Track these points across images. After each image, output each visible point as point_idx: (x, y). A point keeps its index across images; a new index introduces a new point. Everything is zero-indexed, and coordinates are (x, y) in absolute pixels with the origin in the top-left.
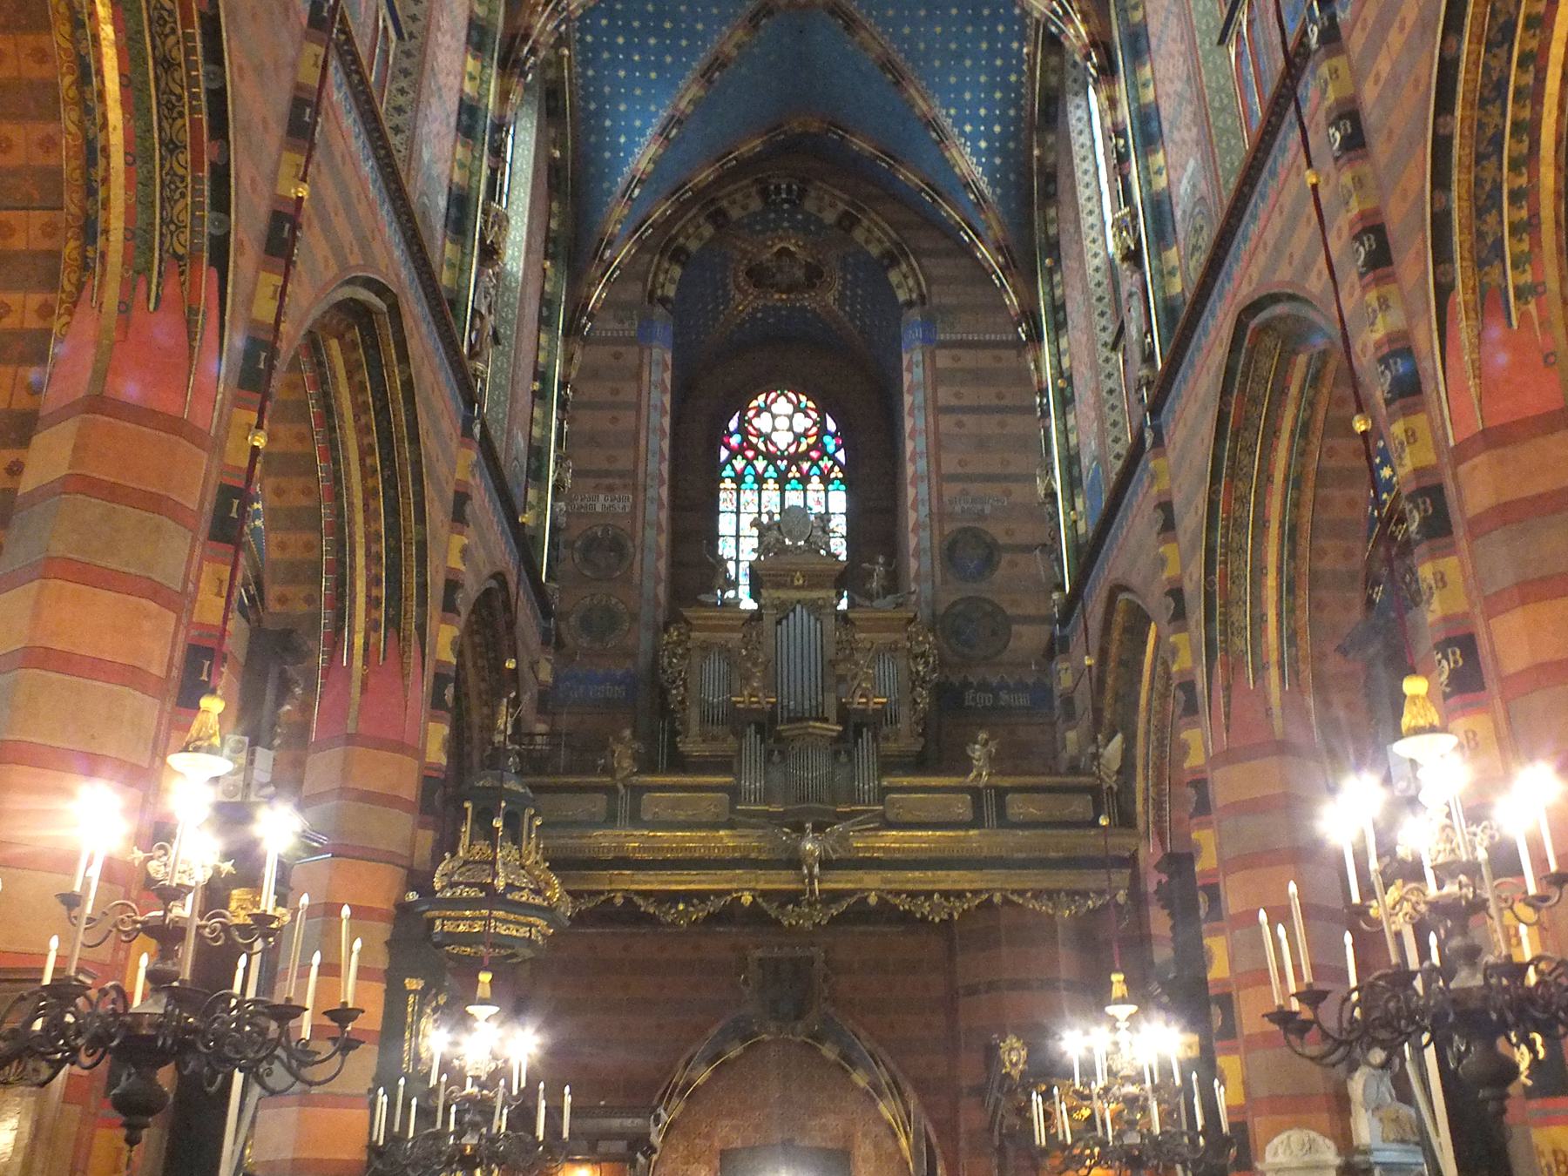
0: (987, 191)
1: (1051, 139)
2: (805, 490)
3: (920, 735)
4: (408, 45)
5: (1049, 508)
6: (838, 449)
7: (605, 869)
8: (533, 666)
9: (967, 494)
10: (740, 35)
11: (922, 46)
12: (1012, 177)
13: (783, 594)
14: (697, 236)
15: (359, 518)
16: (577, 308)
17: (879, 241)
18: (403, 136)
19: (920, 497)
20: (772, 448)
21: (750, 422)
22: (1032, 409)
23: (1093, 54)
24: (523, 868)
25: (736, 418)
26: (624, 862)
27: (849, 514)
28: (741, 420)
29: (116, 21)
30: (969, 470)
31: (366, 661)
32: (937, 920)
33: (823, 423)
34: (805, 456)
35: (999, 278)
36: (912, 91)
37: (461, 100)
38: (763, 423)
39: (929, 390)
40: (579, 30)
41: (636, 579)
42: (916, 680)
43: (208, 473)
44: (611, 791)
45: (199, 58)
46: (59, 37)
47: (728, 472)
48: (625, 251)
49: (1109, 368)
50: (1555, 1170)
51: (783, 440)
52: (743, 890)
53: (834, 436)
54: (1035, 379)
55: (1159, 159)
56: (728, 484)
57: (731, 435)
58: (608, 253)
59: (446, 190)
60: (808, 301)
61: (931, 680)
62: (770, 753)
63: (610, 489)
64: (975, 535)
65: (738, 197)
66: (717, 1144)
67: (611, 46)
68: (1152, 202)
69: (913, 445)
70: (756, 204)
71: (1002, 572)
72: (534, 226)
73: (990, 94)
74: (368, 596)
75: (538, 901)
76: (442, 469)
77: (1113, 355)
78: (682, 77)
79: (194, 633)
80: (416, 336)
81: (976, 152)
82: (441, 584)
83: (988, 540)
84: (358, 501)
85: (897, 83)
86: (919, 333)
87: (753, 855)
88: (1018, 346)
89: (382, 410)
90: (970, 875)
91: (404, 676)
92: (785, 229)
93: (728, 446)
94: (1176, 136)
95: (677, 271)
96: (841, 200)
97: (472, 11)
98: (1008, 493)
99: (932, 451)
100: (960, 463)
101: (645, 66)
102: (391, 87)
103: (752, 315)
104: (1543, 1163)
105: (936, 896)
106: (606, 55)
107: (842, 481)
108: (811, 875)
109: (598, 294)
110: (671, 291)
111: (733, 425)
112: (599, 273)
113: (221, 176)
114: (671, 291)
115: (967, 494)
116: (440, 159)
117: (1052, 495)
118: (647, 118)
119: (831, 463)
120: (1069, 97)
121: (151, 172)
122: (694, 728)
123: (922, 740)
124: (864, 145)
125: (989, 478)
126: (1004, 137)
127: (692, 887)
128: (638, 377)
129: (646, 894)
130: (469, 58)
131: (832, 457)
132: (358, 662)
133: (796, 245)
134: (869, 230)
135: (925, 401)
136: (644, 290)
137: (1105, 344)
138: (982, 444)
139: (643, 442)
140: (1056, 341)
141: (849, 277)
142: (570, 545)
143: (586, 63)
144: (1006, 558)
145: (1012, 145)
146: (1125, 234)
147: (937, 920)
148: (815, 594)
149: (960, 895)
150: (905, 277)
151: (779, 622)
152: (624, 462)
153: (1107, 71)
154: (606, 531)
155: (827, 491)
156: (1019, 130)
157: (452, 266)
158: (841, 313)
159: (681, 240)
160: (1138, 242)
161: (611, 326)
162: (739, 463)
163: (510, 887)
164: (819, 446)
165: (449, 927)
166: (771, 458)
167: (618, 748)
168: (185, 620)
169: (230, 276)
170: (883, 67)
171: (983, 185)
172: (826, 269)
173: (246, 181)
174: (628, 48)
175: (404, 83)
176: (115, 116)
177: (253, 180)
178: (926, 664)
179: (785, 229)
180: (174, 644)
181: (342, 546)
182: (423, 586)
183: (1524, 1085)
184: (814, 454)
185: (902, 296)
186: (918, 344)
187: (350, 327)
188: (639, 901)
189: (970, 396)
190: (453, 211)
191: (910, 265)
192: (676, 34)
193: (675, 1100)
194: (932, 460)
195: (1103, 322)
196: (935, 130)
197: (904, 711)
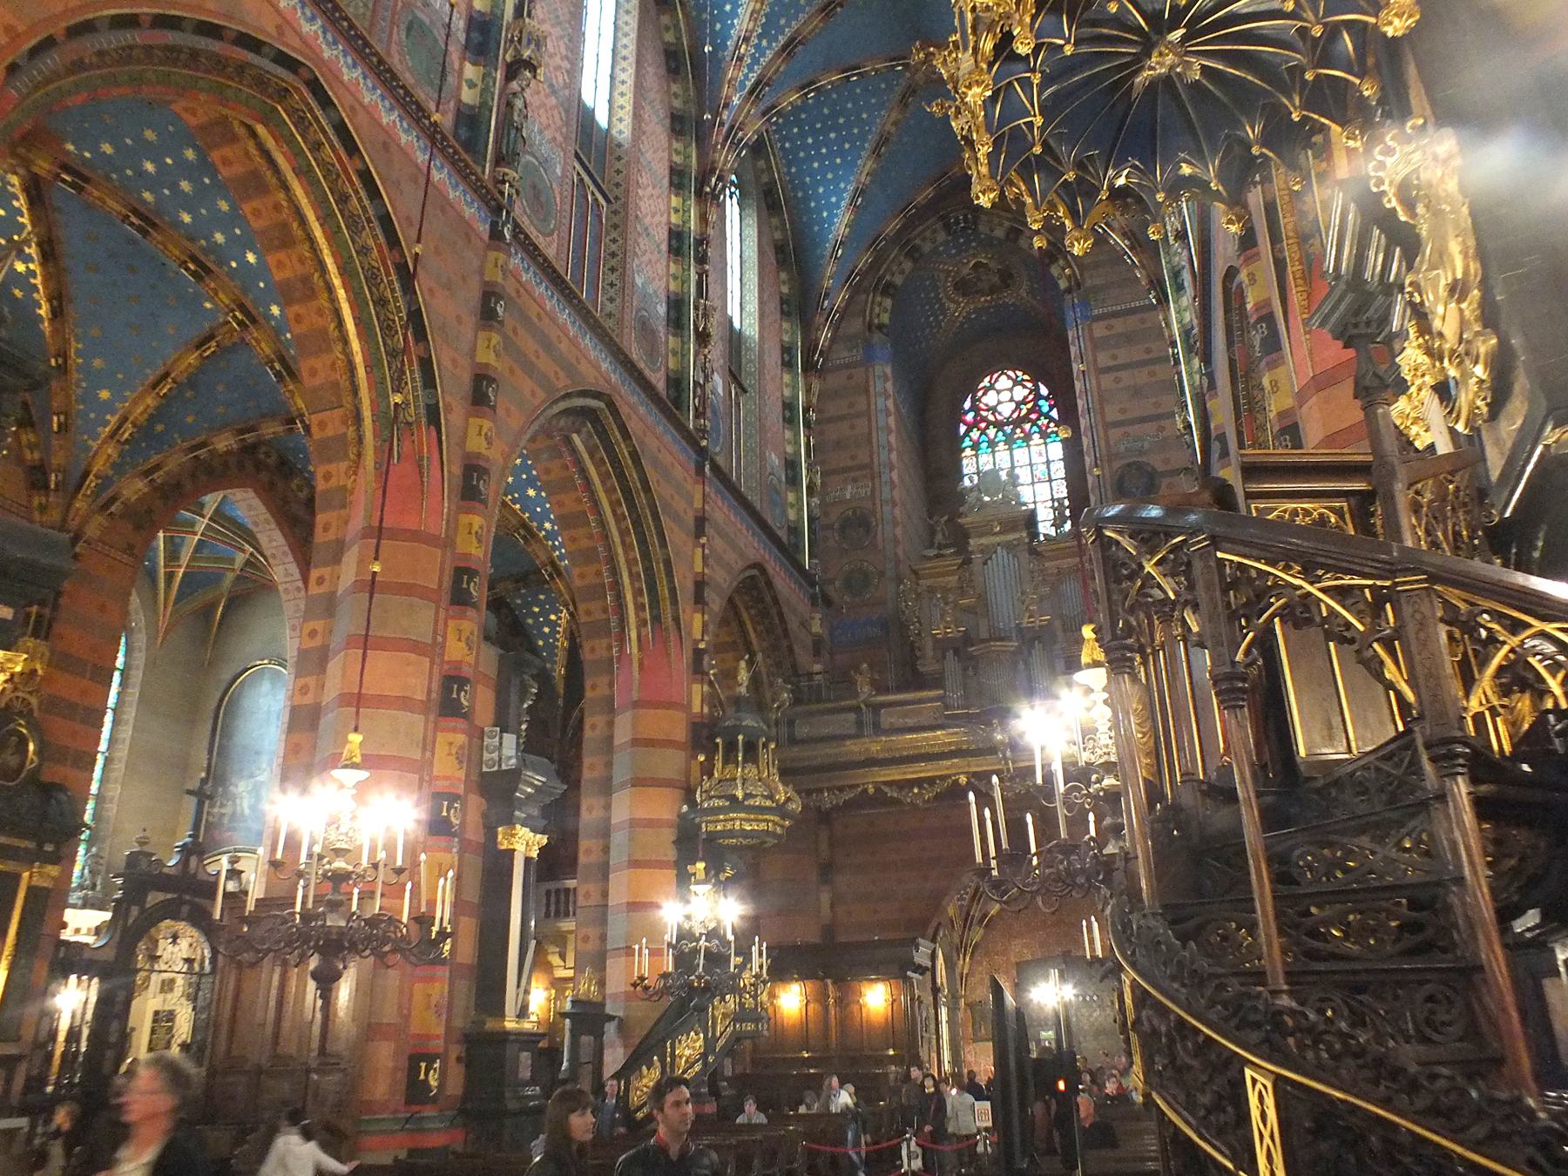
2: (1028, 446)
4: (616, 206)
6: (1050, 410)
7: (860, 768)
8: (804, 624)
10: (894, 115)
13: (984, 541)
14: (899, 272)
15: (620, 550)
16: (810, 347)
18: (618, 273)
20: (999, 417)
21: (979, 400)
22: (1167, 359)
24: (760, 780)
25: (969, 399)
26: (872, 762)
28: (974, 401)
29: (345, 286)
30: (1129, 416)
31: (640, 649)
33: (1037, 389)
34: (1026, 419)
35: (1130, 257)
37: (670, 229)
38: (990, 399)
40: (779, 140)
41: (880, 547)
43: (443, 563)
44: (857, 709)
45: (398, 294)
46: (323, 300)
47: (967, 442)
48: (841, 298)
51: (1006, 410)
52: (958, 774)
53: (1047, 399)
56: (968, 452)
57: (967, 412)
58: (826, 303)
59: (664, 299)
60: (1008, 298)
62: (965, 669)
63: (855, 480)
64: (1139, 466)
65: (928, 234)
66: (1013, 959)
67: (805, 147)
70: (941, 236)
72: (765, 298)
74: (635, 604)
75: (768, 803)
76: (679, 504)
78: (860, 157)
79: (446, 667)
80: (634, 416)
82: (690, 585)
84: (617, 539)
87: (964, 747)
88: (1152, 307)
89: (621, 477)
91: (668, 655)
92: (975, 248)
93: (965, 423)
95: (888, 302)
96: (1007, 219)
97: (670, 161)
101: (831, 155)
102: (605, 240)
103: (967, 318)
106: (802, 154)
108: (1005, 758)
109: (824, 336)
110: (885, 318)
111: (967, 405)
112: (822, 320)
113: (426, 365)
114: (885, 318)
116: (654, 279)
118: (839, 193)
121: (384, 374)
122: (929, 652)
127: (922, 775)
128: (867, 391)
129: (889, 784)
130: (673, 197)
131: (1047, 416)
132: (635, 650)
133: (986, 258)
136: (864, 322)
138: (1137, 392)
139: (874, 440)
142: (830, 527)
143: (789, 164)
144: (1165, 482)
148: (1010, 537)
151: (985, 563)
152: (863, 457)
154: (854, 512)
155: (1045, 443)
157: (675, 354)
159: (888, 277)
161: (843, 355)
162: (975, 434)
163: (747, 796)
164: (1036, 409)
165: (711, 828)
166: (999, 425)
167: (859, 678)
168: (437, 660)
169: (443, 429)
172: (1014, 271)
173: (447, 363)
174: (817, 146)
175: (614, 235)
176: (355, 345)
177: (454, 361)
179: (975, 248)
180: (430, 679)
181: (615, 572)
182: (673, 590)
184: (1033, 416)
185: (1063, 284)
187: (584, 424)
188: (886, 789)
189: (1124, 356)
190: (672, 313)
192: (848, 126)
193: (975, 928)
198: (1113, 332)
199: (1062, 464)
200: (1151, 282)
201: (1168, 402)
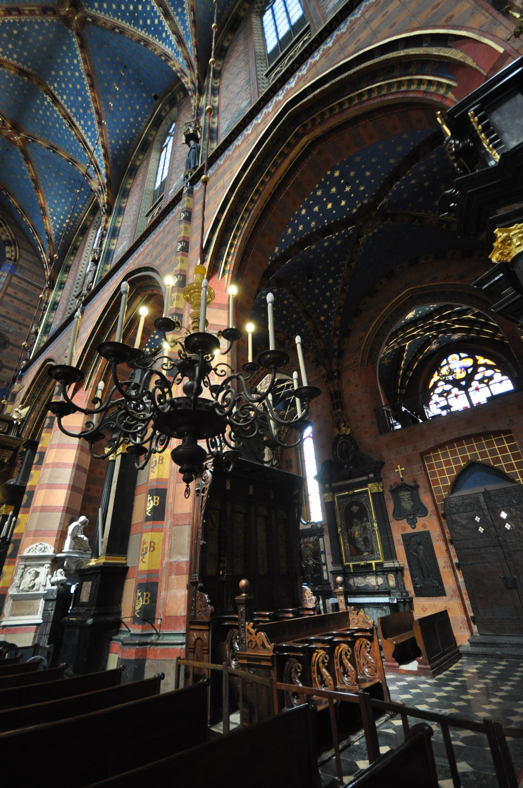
1: (81, 238)
17: (7, 236)
30: (9, 316)
39: (5, 286)
49: (72, 302)
50: (148, 549)
71: (8, 350)
77: (75, 299)
81: (54, 226)
83: (7, 339)
86: (9, 268)
94: (123, 236)
104: (145, 546)
117: (36, 333)
120: (92, 229)
125: (15, 321)
137: (74, 296)
138: (18, 311)
144: (10, 347)
150: (12, 251)
153: (109, 212)
183: (147, 515)
185: (8, 255)
189: (20, 295)
195: (76, 289)
196: (43, 210)
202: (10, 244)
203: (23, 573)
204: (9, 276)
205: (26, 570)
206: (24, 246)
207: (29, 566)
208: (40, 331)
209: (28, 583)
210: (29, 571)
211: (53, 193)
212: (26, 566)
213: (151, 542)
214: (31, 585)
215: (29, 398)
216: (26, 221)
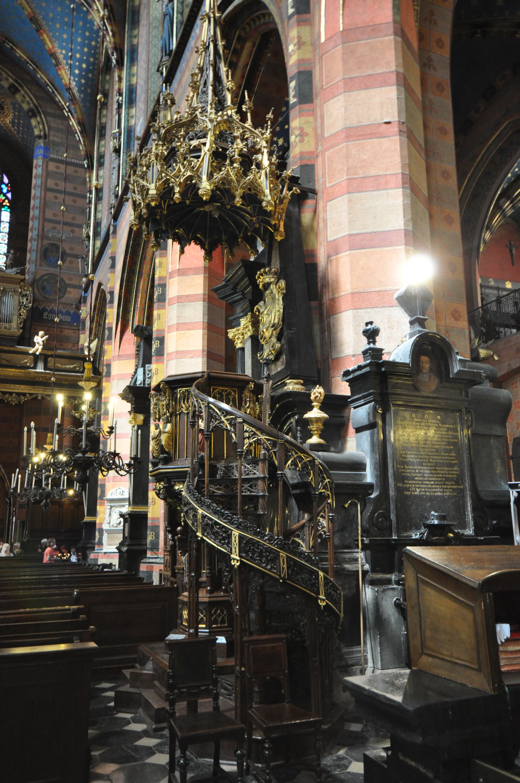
0: (77, 95)
3: (21, 328)
5: (86, 242)
9: (55, 229)
11: (51, 15)
12: (89, 91)
19: (34, 227)
23: (115, 54)
27: (11, 223)
32: (14, 404)
36: (45, 36)
42: (21, 304)
53: (7, 185)
54: (88, 185)
55: (133, 111)
61: (28, 307)
68: (128, 129)
69: (34, 203)
73: (82, 49)
85: (38, 31)
90: (28, 387)
98: (73, 232)
99: (42, 206)
100: (54, 214)
105: (14, 394)
107: (9, 207)
115: (55, 229)
117: (88, 237)
119: (4, 198)
123: (21, 331)
124: (23, 55)
126: (87, 70)
134: (24, 97)
135: (42, 183)
140: (97, 171)
141: (17, 113)
145: (90, 75)
146: (115, 141)
147: (14, 404)
149: (24, 394)
150: (38, 123)
156: (94, 69)
158: (13, 129)
160: (120, 146)
170: (31, 19)
171: (75, 90)
178: (27, 299)
185: (36, 132)
186: (41, 157)
189: (61, 185)
191: (41, 118)
194: (42, 209)
196: (54, 59)
197: (15, 318)
198: (59, 171)
199: (7, 225)
200: (87, 155)
201: (79, 218)
202: (34, 116)
203: (110, 513)
204: (45, 163)
205: (112, 509)
206: (49, 110)
207: (114, 506)
208: (91, 234)
209: (116, 520)
210: (114, 511)
211: (58, 26)
212: (111, 507)
213: (152, 499)
214: (118, 522)
215: (96, 328)
216: (41, 77)
